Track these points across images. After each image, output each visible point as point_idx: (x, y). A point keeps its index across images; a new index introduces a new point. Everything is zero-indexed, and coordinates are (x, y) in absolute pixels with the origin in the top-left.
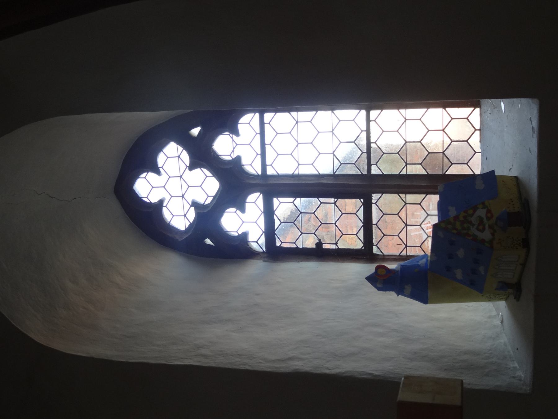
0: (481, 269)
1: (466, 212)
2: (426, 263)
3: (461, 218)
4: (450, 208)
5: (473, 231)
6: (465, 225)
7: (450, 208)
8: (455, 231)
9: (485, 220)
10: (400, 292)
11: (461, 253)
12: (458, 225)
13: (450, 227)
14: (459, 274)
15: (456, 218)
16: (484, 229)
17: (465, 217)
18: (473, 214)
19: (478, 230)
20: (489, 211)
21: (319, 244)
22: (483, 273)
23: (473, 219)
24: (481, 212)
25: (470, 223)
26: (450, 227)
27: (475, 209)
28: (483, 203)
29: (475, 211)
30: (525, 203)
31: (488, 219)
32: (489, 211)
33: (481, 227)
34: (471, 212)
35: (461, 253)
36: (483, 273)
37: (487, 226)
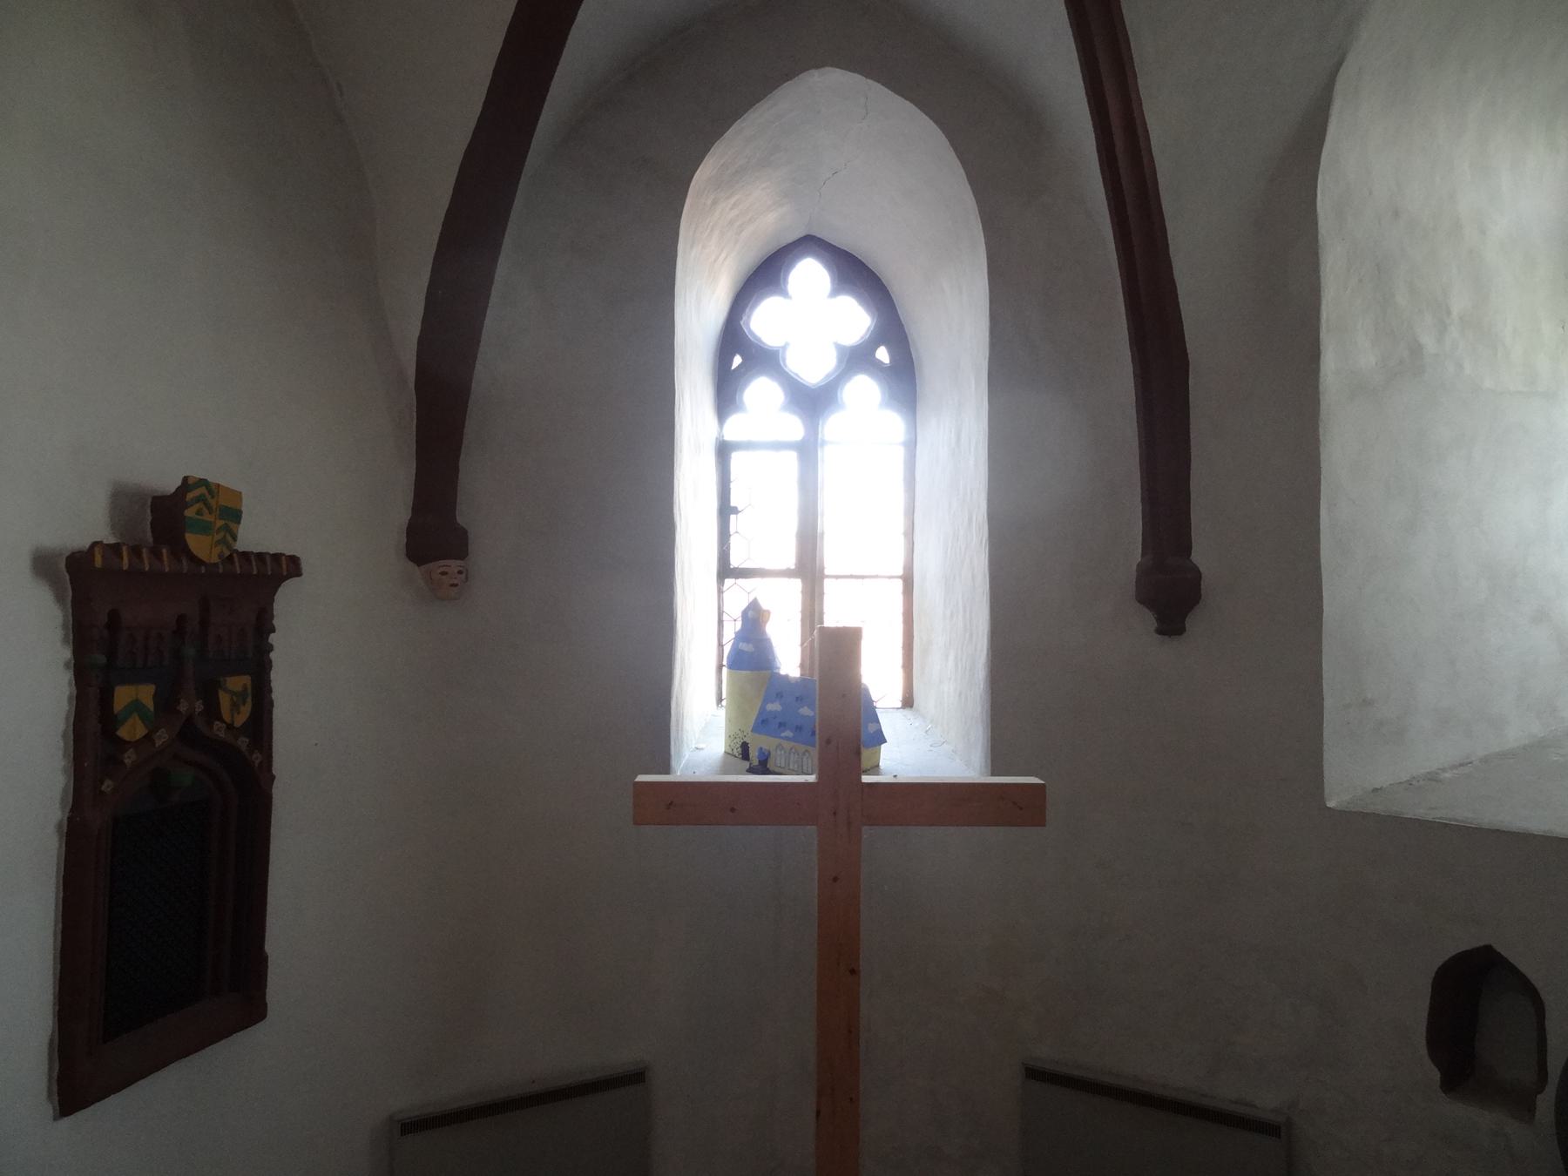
0: (788, 733)
14: (774, 707)
21: (735, 511)
22: (783, 735)
36: (783, 735)
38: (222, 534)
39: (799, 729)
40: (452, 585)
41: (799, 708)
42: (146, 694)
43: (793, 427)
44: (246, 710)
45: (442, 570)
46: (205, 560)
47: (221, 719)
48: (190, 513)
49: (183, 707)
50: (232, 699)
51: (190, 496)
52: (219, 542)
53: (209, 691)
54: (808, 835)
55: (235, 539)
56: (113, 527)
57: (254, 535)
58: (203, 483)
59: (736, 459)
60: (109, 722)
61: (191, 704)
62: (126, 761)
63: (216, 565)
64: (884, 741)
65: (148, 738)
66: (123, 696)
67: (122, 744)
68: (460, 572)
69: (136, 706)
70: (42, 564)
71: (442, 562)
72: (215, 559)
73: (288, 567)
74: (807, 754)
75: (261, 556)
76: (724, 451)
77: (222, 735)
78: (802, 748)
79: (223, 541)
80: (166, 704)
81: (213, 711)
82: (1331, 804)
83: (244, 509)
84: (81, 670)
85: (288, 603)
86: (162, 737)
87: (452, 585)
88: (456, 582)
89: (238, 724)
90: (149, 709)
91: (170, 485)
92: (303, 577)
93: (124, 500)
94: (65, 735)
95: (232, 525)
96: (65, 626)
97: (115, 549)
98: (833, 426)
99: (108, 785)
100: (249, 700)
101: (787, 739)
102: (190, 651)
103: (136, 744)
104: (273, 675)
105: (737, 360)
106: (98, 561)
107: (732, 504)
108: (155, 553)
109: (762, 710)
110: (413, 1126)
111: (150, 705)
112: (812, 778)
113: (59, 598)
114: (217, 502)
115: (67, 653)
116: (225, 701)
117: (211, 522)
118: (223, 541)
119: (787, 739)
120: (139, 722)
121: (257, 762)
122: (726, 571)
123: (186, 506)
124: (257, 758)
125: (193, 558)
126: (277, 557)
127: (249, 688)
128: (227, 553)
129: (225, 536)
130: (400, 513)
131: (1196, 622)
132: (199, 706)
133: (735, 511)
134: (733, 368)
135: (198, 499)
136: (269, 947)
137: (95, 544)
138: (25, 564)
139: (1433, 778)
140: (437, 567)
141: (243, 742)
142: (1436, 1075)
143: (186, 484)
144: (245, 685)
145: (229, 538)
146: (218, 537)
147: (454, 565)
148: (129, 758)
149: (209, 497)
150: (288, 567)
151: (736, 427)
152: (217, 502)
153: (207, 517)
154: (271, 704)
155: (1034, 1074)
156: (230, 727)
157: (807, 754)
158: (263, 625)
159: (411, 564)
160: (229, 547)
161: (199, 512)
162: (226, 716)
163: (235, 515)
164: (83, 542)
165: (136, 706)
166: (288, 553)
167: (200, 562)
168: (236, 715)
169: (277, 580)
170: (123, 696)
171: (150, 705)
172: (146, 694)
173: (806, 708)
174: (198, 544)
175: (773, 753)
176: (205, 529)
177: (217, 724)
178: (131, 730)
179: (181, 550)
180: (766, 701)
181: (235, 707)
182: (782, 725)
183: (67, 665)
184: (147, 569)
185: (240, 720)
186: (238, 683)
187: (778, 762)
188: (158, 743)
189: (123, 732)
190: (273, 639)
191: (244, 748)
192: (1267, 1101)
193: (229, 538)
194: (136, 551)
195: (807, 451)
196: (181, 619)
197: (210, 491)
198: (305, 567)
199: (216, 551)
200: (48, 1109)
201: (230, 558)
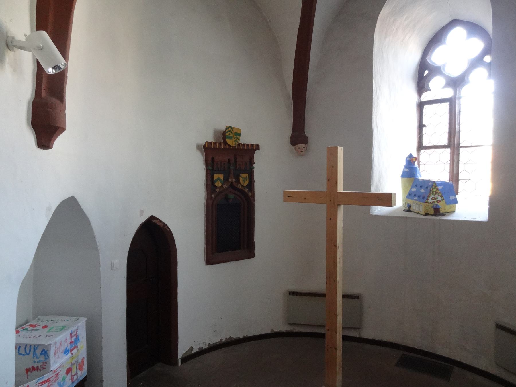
0: (416, 198)
1: (440, 193)
2: (418, 177)
3: (437, 191)
4: (442, 186)
5: (432, 196)
6: (434, 193)
7: (442, 186)
8: (432, 189)
9: (436, 200)
10: (406, 167)
11: (422, 191)
12: (435, 190)
13: (434, 187)
14: (414, 189)
15: (438, 189)
16: (433, 200)
17: (438, 193)
18: (439, 195)
19: (432, 198)
20: (440, 201)
21: (425, 126)
22: (415, 199)
23: (437, 196)
24: (440, 198)
25: (435, 195)
26: (434, 187)
27: (442, 196)
28: (443, 199)
29: (440, 196)
30: (443, 215)
31: (437, 201)
32: (440, 201)
33: (433, 198)
34: (440, 195)
35: (422, 191)
36: (415, 199)
37: (434, 201)
38: (235, 139)
39: (419, 196)
40: (301, 151)
41: (421, 190)
42: (221, 176)
43: (449, 93)
45: (298, 147)
46: (231, 145)
47: (240, 184)
49: (230, 180)
50: (243, 179)
52: (235, 141)
53: (237, 177)
55: (239, 140)
56: (214, 138)
61: (232, 180)
63: (235, 146)
64: (457, 203)
65: (222, 186)
66: (216, 176)
67: (216, 187)
68: (304, 148)
69: (219, 179)
70: (198, 147)
71: (298, 145)
72: (234, 145)
74: (421, 205)
75: (248, 145)
76: (421, 106)
77: (240, 187)
78: (419, 203)
79: (236, 141)
80: (226, 179)
81: (238, 182)
83: (241, 133)
84: (207, 170)
85: (257, 156)
86: (225, 187)
87: (301, 151)
88: (302, 150)
90: (222, 180)
92: (260, 150)
93: (216, 132)
94: (205, 184)
95: (238, 137)
96: (204, 161)
98: (465, 91)
101: (415, 200)
102: (232, 167)
104: (255, 174)
105: (426, 72)
106: (207, 146)
107: (424, 124)
109: (410, 191)
110: (292, 293)
111: (223, 179)
113: (202, 154)
114: (234, 132)
115: (204, 166)
116: (241, 180)
117: (232, 137)
118: (236, 141)
119: (415, 200)
121: (250, 195)
124: (250, 194)
125: (229, 145)
126: (252, 145)
127: (248, 177)
128: (237, 144)
129: (236, 140)
130: (289, 133)
132: (234, 180)
133: (425, 126)
134: (424, 76)
135: (229, 131)
136: (255, 241)
141: (246, 190)
144: (246, 177)
146: (234, 140)
147: (302, 146)
148: (218, 190)
149: (232, 131)
151: (426, 97)
152: (234, 132)
153: (231, 135)
155: (499, 327)
156: (243, 186)
157: (421, 205)
158: (251, 162)
160: (238, 142)
161: (229, 134)
162: (242, 183)
163: (239, 135)
165: (219, 179)
166: (251, 143)
167: (231, 146)
168: (244, 183)
170: (216, 176)
171: (222, 179)
172: (221, 176)
173: (423, 190)
174: (229, 141)
175: (412, 205)
176: (231, 138)
177: (239, 185)
178: (218, 184)
179: (225, 143)
180: (411, 188)
181: (244, 181)
182: (415, 195)
184: (218, 147)
185: (245, 184)
186: (245, 175)
187: (413, 208)
188: (224, 188)
189: (216, 184)
190: (254, 165)
193: (237, 140)
194: (220, 144)
195: (452, 102)
196: (229, 160)
198: (260, 147)
200: (204, 263)
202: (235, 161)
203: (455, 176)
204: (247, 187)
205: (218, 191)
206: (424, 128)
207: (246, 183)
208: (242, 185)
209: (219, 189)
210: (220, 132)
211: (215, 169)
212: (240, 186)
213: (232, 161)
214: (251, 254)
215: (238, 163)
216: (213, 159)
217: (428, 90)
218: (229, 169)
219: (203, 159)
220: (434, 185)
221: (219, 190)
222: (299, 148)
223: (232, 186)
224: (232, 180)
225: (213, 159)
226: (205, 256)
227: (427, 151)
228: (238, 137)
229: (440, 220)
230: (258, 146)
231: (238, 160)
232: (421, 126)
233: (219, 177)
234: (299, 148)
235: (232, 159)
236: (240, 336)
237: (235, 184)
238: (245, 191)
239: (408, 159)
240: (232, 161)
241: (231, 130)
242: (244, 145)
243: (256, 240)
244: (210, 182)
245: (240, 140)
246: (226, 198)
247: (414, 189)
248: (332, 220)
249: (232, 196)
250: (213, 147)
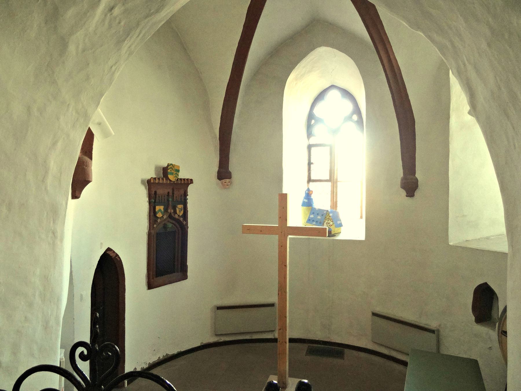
0: (314, 223)
1: (332, 219)
2: (314, 206)
3: (330, 218)
4: (332, 214)
5: (326, 221)
6: (328, 219)
7: (332, 214)
8: (326, 216)
9: (329, 224)
10: (305, 198)
11: (319, 217)
12: (328, 217)
13: (328, 215)
14: (312, 216)
15: (330, 216)
16: (327, 224)
17: (330, 219)
18: (331, 221)
19: (327, 223)
20: (332, 225)
21: (312, 163)
22: (313, 223)
23: (329, 221)
24: (331, 223)
25: (329, 220)
26: (328, 215)
27: (332, 222)
28: (334, 224)
29: (332, 221)
30: (334, 235)
31: (330, 225)
32: (332, 225)
33: (327, 223)
34: (332, 220)
35: (319, 217)
36: (313, 223)
37: (327, 225)
42: (162, 208)
44: (182, 212)
45: (225, 182)
47: (177, 214)
48: (169, 171)
49: (169, 211)
51: (169, 167)
53: (174, 208)
54: (276, 237)
55: (178, 176)
56: (156, 174)
57: (182, 175)
58: (171, 164)
59: (313, 149)
60: (155, 213)
61: (171, 210)
62: (158, 221)
63: (175, 181)
65: (162, 217)
66: (158, 208)
68: (229, 182)
69: (160, 210)
70: (143, 182)
71: (225, 180)
72: (174, 180)
73: (190, 181)
75: (184, 179)
76: (310, 147)
80: (166, 210)
81: (175, 212)
82: (451, 244)
83: (180, 169)
84: (150, 203)
86: (165, 217)
88: (228, 184)
89: (181, 215)
91: (166, 165)
93: (157, 168)
94: (147, 215)
95: (178, 173)
96: (147, 194)
97: (155, 178)
99: (155, 226)
100: (183, 211)
102: (170, 199)
103: (160, 218)
105: (313, 122)
107: (312, 162)
108: (163, 179)
109: (309, 217)
110: (219, 308)
112: (278, 225)
113: (146, 188)
115: (147, 199)
116: (177, 209)
120: (161, 214)
122: (310, 180)
123: (168, 169)
124: (185, 223)
125: (170, 180)
126: (188, 179)
128: (177, 179)
130: (216, 169)
131: (417, 193)
132: (172, 211)
133: (312, 163)
134: (312, 124)
135: (170, 168)
137: (151, 178)
138: (140, 181)
139: (488, 238)
140: (224, 181)
141: (181, 219)
142: (474, 318)
143: (168, 165)
145: (177, 176)
147: (228, 180)
148: (159, 220)
150: (190, 181)
153: (172, 171)
154: (188, 211)
155: (374, 314)
156: (179, 216)
158: (186, 194)
159: (218, 180)
160: (177, 178)
161: (171, 171)
162: (178, 213)
164: (149, 178)
165: (160, 210)
169: (188, 185)
172: (162, 208)
174: (171, 177)
176: (172, 174)
178: (159, 215)
179: (167, 178)
180: (310, 215)
182: (313, 221)
183: (147, 202)
186: (180, 206)
189: (158, 215)
190: (188, 197)
191: (182, 220)
192: (433, 324)
193: (177, 176)
194: (159, 179)
196: (168, 193)
197: (173, 166)
199: (174, 179)
201: (178, 180)
202: (173, 194)
203: (334, 205)
204: (182, 216)
205: (160, 221)
206: (312, 165)
207: (181, 213)
208: (179, 215)
209: (160, 219)
210: (160, 168)
211: (157, 201)
212: (176, 216)
213: (171, 194)
214: (184, 277)
215: (175, 196)
216: (155, 192)
217: (313, 135)
218: (168, 201)
219: (146, 193)
220: (328, 213)
221: (160, 220)
222: (225, 182)
223: (170, 216)
224: (171, 210)
225: (155, 192)
226: (147, 282)
227: (314, 183)
228: (178, 173)
229: (333, 240)
230: (191, 180)
231: (175, 193)
232: (310, 164)
233: (160, 208)
234: (225, 182)
235: (171, 191)
236: (175, 352)
237: (173, 215)
238: (180, 221)
239: (307, 192)
240: (171, 194)
241: (172, 167)
242: (181, 179)
243: (188, 264)
244: (152, 214)
245: (179, 176)
246: (165, 227)
247: (312, 216)
248: (282, 247)
249: (170, 225)
250: (157, 182)
